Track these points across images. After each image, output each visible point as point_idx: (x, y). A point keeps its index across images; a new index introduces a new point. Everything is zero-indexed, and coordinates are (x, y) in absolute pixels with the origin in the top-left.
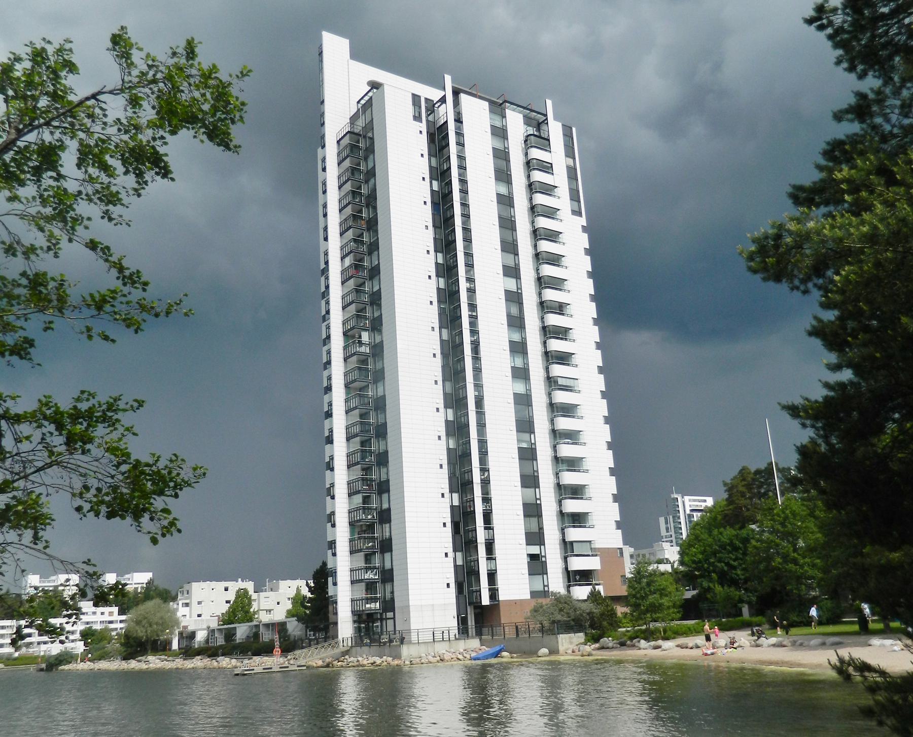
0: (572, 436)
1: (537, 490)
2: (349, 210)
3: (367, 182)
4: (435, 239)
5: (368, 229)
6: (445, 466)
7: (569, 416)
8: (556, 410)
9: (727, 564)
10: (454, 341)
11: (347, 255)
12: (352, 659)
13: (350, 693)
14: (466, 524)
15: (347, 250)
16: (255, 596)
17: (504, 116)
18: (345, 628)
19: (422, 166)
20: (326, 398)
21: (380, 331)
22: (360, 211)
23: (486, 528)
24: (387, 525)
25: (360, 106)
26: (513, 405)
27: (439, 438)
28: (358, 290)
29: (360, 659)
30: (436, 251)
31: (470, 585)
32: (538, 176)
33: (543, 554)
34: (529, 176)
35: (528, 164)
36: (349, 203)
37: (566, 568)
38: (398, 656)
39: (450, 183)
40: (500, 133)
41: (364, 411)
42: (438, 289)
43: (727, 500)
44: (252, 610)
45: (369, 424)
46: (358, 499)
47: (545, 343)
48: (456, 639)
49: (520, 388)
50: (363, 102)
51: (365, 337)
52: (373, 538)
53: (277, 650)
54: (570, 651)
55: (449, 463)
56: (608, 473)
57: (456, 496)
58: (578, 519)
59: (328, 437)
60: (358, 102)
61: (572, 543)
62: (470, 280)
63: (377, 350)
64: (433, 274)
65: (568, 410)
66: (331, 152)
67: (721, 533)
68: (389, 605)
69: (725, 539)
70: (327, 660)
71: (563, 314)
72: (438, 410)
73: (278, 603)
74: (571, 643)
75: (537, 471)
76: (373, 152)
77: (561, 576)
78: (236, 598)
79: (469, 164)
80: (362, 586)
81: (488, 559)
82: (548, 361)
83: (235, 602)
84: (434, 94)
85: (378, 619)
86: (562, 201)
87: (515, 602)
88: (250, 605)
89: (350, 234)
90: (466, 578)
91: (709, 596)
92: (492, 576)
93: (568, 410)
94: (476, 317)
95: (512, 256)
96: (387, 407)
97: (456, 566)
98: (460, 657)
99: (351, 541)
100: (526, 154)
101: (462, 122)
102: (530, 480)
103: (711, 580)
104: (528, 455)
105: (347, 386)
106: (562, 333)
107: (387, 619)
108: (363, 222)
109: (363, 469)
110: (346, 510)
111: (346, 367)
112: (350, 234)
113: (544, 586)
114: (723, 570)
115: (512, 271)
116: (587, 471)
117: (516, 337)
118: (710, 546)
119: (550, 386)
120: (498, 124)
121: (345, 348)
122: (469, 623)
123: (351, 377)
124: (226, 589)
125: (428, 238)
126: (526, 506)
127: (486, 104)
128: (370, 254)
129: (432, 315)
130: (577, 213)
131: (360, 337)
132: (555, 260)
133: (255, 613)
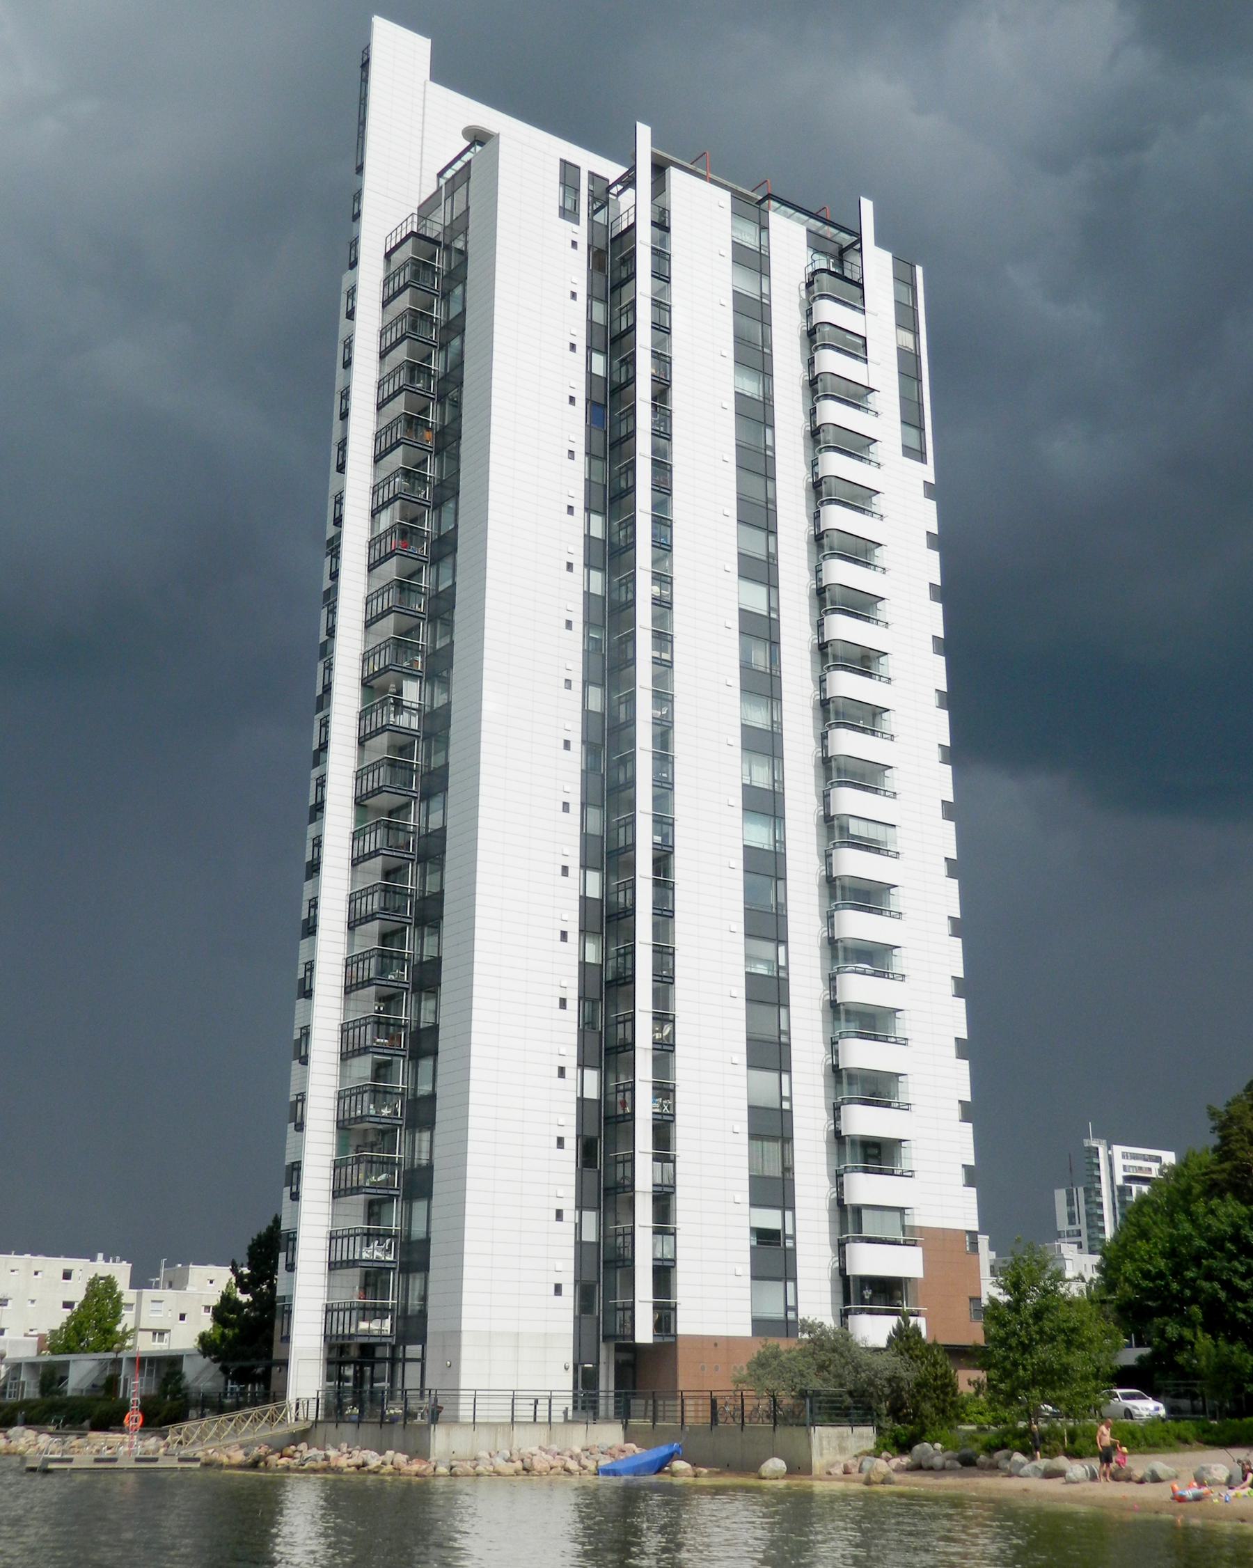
0: (874, 957)
1: (785, 1077)
2: (398, 406)
3: (444, 346)
4: (589, 482)
5: (438, 452)
6: (573, 1004)
7: (870, 910)
8: (843, 893)
9: (1227, 1285)
10: (613, 717)
11: (385, 505)
12: (314, 1451)
13: (301, 1531)
14: (611, 1145)
15: (385, 494)
16: (129, 1296)
17: (764, 227)
18: (305, 1376)
19: (573, 319)
20: (311, 831)
21: (446, 683)
22: (425, 411)
23: (656, 1158)
24: (426, 1136)
25: (442, 181)
26: (740, 874)
27: (564, 935)
28: (404, 586)
29: (332, 1453)
30: (588, 510)
31: (610, 1292)
32: (831, 361)
33: (789, 1231)
34: (811, 363)
35: (811, 334)
36: (401, 390)
37: (842, 1270)
38: (420, 1452)
39: (630, 361)
40: (753, 261)
41: (396, 862)
42: (588, 595)
43: (1215, 1150)
44: (119, 1328)
45: (403, 893)
46: (363, 1068)
47: (824, 737)
48: (566, 1421)
49: (761, 836)
50: (449, 174)
51: (411, 692)
52: (389, 1164)
53: (134, 1418)
54: (838, 1471)
55: (582, 998)
56: (952, 1051)
57: (592, 1076)
58: (878, 1154)
59: (307, 921)
60: (440, 175)
61: (858, 1210)
62: (662, 578)
63: (437, 725)
64: (579, 561)
65: (870, 897)
66: (370, 278)
67: (1212, 1212)
68: (413, 1327)
69: (1221, 1225)
70: (256, 1452)
71: (870, 675)
72: (565, 870)
73: (182, 1317)
74: (842, 1450)
75: (788, 1033)
76: (463, 281)
77: (827, 1286)
78: (87, 1297)
79: (679, 321)
80: (353, 1277)
81: (657, 1232)
82: (828, 778)
83: (82, 1306)
84: (612, 171)
85: (383, 1360)
86: (883, 422)
87: (715, 1343)
88: (116, 1316)
89: (396, 459)
90: (602, 1274)
91: (1181, 1359)
92: (664, 1273)
93: (870, 897)
94: (669, 665)
95: (761, 535)
96: (449, 855)
97: (580, 1245)
98: (573, 1465)
99: (338, 1166)
100: (809, 313)
101: (668, 230)
102: (769, 1053)
103: (1188, 1322)
104: (767, 993)
105: (360, 803)
106: (868, 718)
107: (405, 1360)
108: (428, 435)
109: (381, 999)
110: (332, 1092)
111: (361, 759)
112: (396, 459)
113: (787, 1308)
114: (1214, 1298)
115: (760, 569)
116: (904, 1042)
117: (759, 718)
118: (1189, 1238)
119: (830, 837)
120: (749, 237)
121: (363, 715)
122: (602, 1386)
123: (369, 784)
124: (67, 1275)
125: (573, 478)
126: (752, 1109)
127: (727, 195)
128: (438, 506)
129: (568, 652)
130: (918, 454)
131: (400, 692)
132: (860, 552)
133: (126, 1335)
